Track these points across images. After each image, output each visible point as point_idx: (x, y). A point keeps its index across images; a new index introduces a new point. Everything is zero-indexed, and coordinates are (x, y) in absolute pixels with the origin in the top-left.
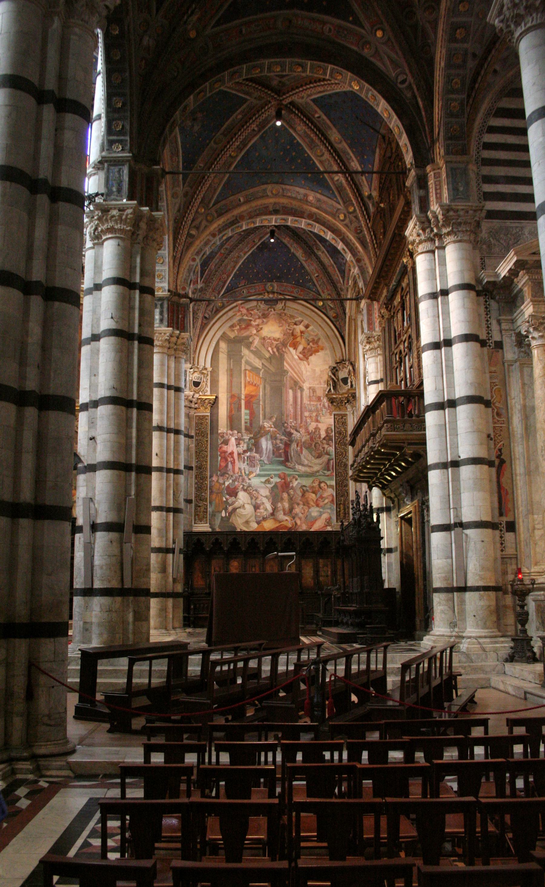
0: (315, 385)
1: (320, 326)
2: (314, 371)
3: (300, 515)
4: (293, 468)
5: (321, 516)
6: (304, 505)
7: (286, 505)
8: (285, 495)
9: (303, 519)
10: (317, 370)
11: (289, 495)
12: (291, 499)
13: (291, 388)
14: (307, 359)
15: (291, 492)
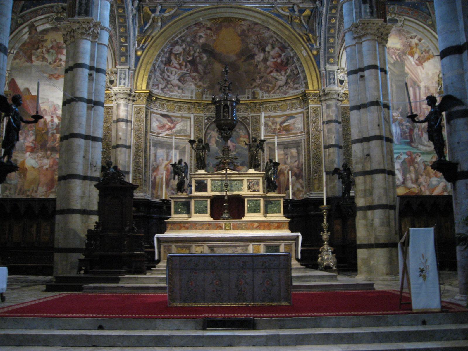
0: (429, 84)
1: (430, 40)
2: (427, 74)
3: (424, 184)
4: (417, 148)
5: (439, 184)
6: (426, 176)
7: (413, 176)
8: (412, 168)
9: (426, 186)
10: (430, 73)
11: (415, 168)
12: (416, 171)
13: (411, 86)
14: (422, 64)
15: (416, 166)
